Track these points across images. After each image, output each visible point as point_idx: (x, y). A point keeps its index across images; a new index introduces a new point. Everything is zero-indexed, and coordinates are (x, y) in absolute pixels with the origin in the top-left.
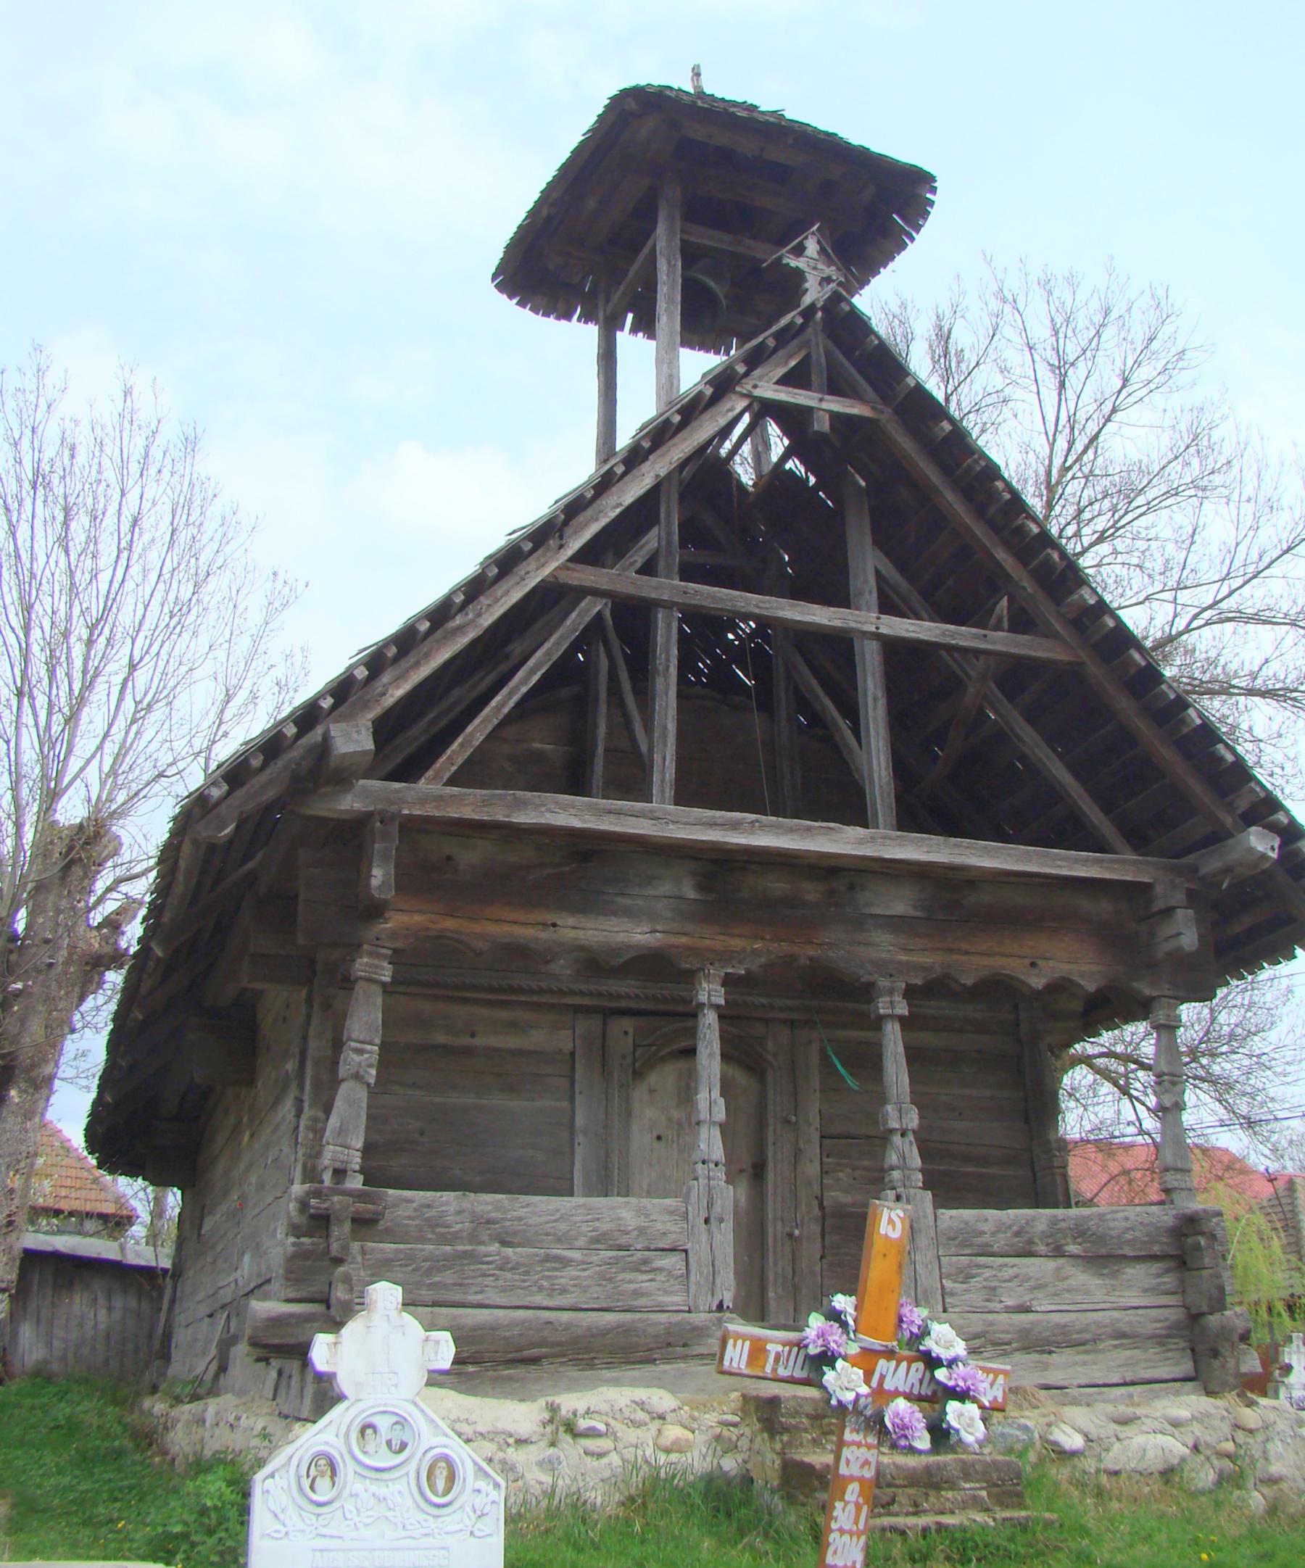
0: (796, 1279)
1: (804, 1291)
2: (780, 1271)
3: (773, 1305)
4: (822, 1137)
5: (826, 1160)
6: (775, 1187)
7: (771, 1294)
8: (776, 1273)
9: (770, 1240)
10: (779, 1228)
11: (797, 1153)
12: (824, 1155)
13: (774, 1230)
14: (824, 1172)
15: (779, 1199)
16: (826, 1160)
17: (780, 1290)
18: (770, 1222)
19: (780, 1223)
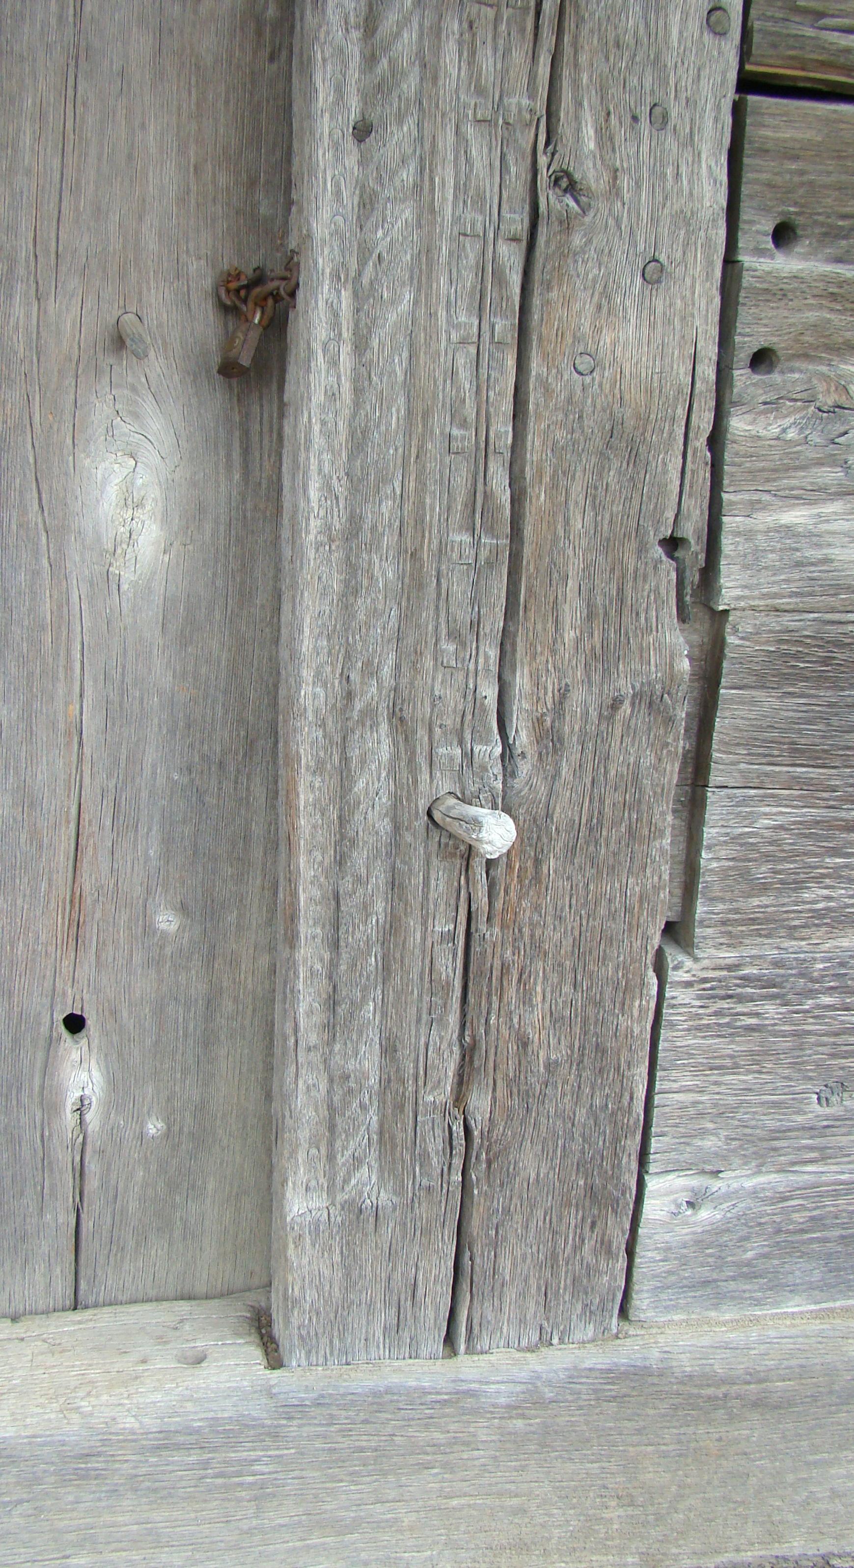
0: (480, 1103)
1: (529, 1163)
2: (368, 1062)
3: (307, 1270)
4: (748, 84)
5: (763, 264)
6: (360, 484)
7: (301, 1204)
8: (339, 1079)
9: (309, 868)
10: (373, 786)
11: (547, 207)
12: (758, 226)
13: (338, 790)
14: (740, 359)
15: (385, 571)
16: (763, 264)
17: (368, 1183)
18: (306, 742)
19: (380, 744)
